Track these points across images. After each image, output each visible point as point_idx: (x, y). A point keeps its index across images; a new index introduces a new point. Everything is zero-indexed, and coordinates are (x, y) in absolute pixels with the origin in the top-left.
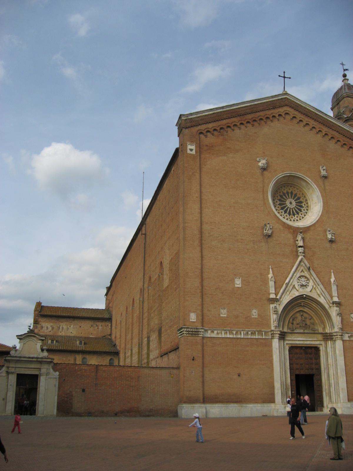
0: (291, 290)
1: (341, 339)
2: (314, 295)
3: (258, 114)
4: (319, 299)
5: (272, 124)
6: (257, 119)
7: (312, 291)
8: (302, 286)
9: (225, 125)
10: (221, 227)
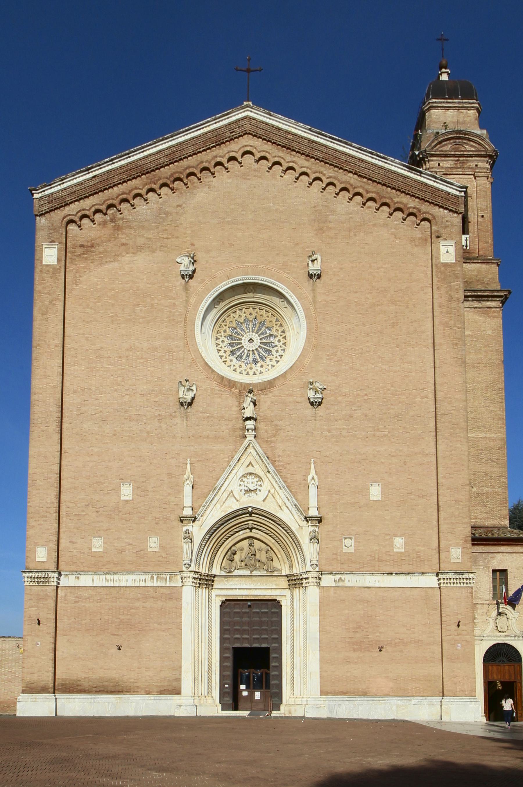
0: (224, 500)
1: (316, 584)
2: (270, 507)
3: (185, 163)
4: (280, 515)
5: (214, 182)
6: (182, 176)
7: (267, 500)
8: (249, 491)
9: (117, 197)
10: (101, 397)
